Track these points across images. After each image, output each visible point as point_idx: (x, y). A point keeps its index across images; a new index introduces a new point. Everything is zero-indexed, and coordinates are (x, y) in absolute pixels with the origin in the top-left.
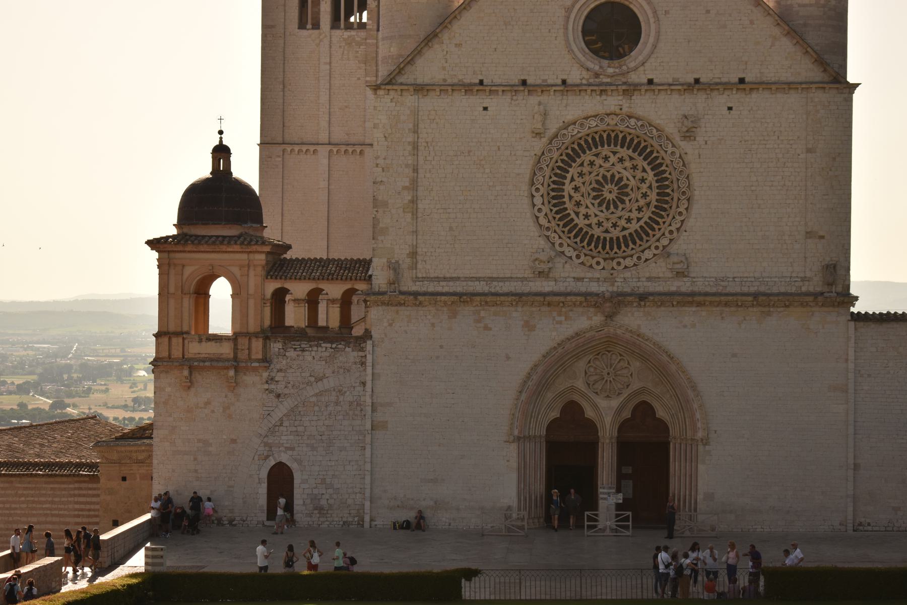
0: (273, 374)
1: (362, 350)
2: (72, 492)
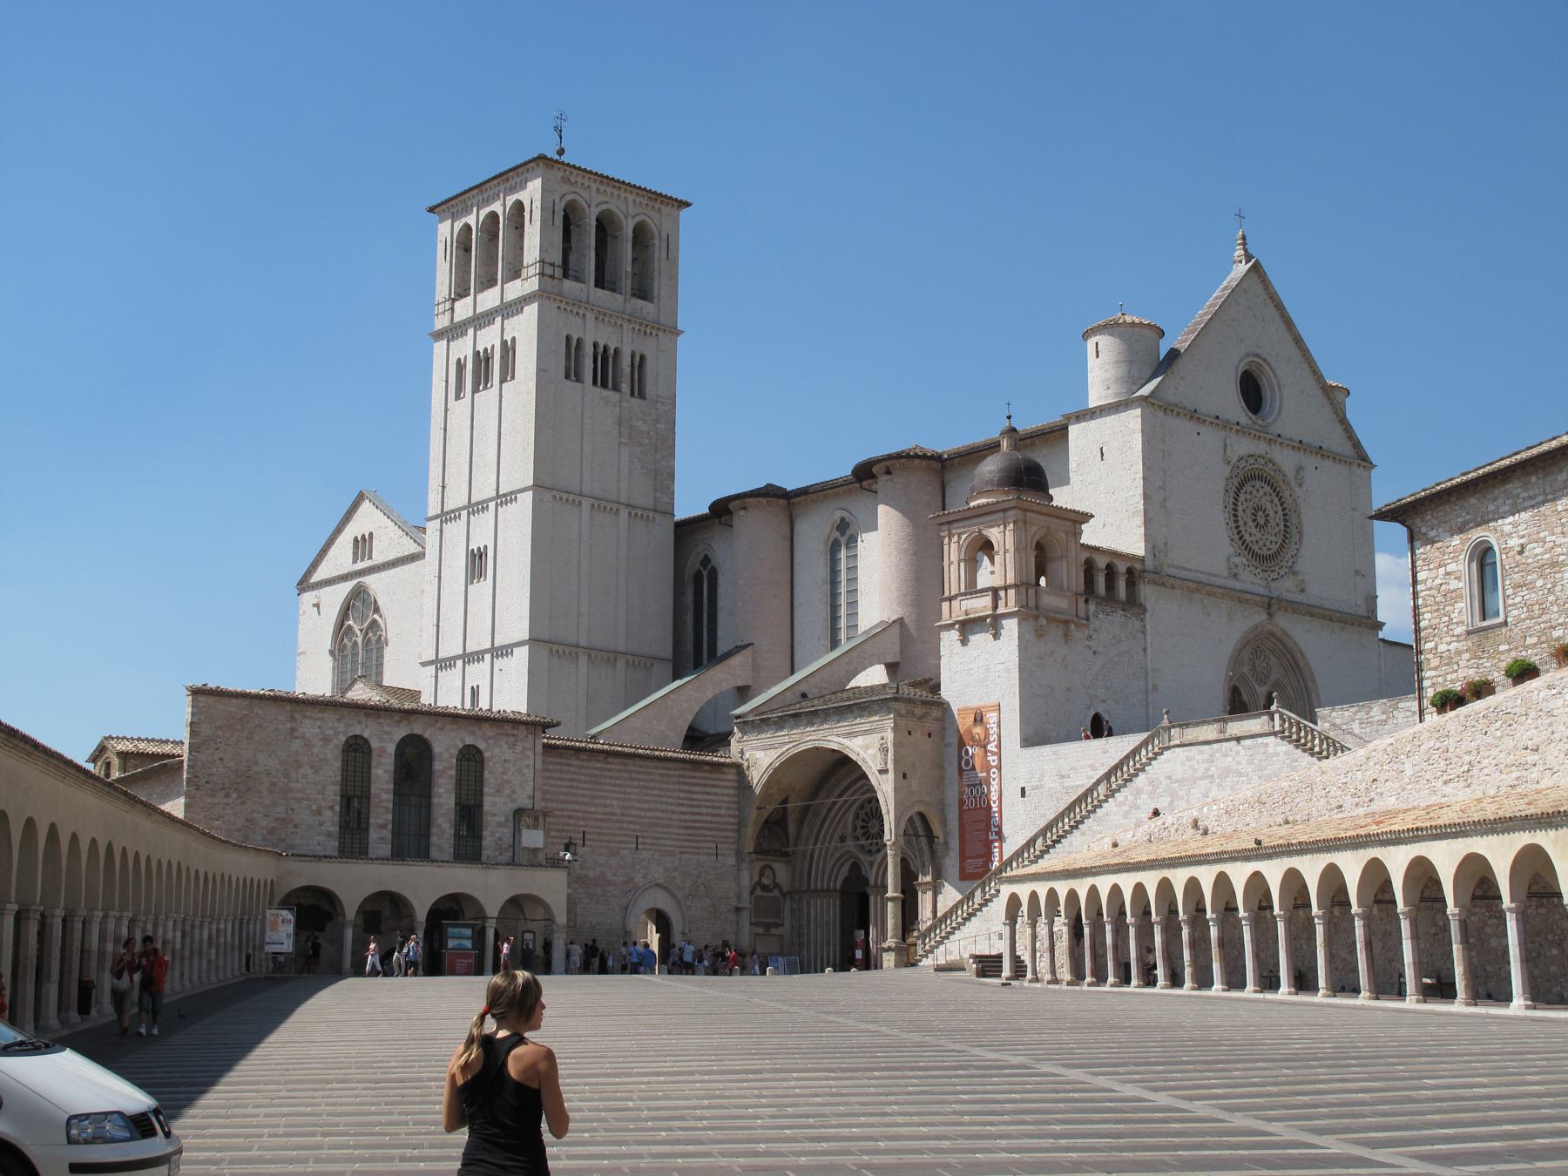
0: (1091, 632)
1: (1142, 620)
2: (677, 780)
